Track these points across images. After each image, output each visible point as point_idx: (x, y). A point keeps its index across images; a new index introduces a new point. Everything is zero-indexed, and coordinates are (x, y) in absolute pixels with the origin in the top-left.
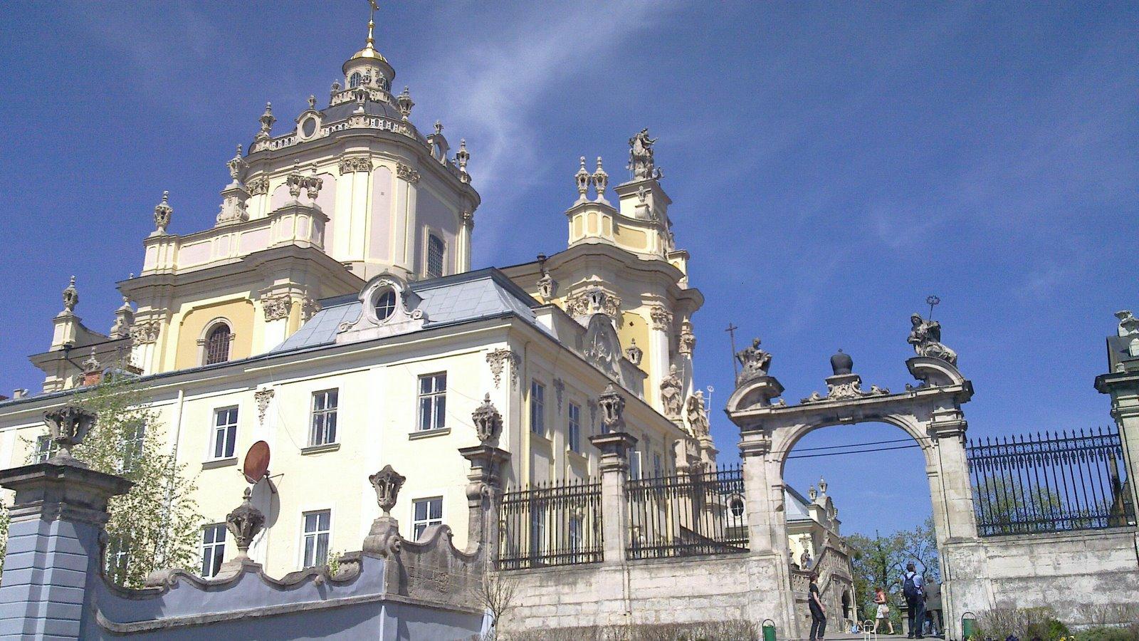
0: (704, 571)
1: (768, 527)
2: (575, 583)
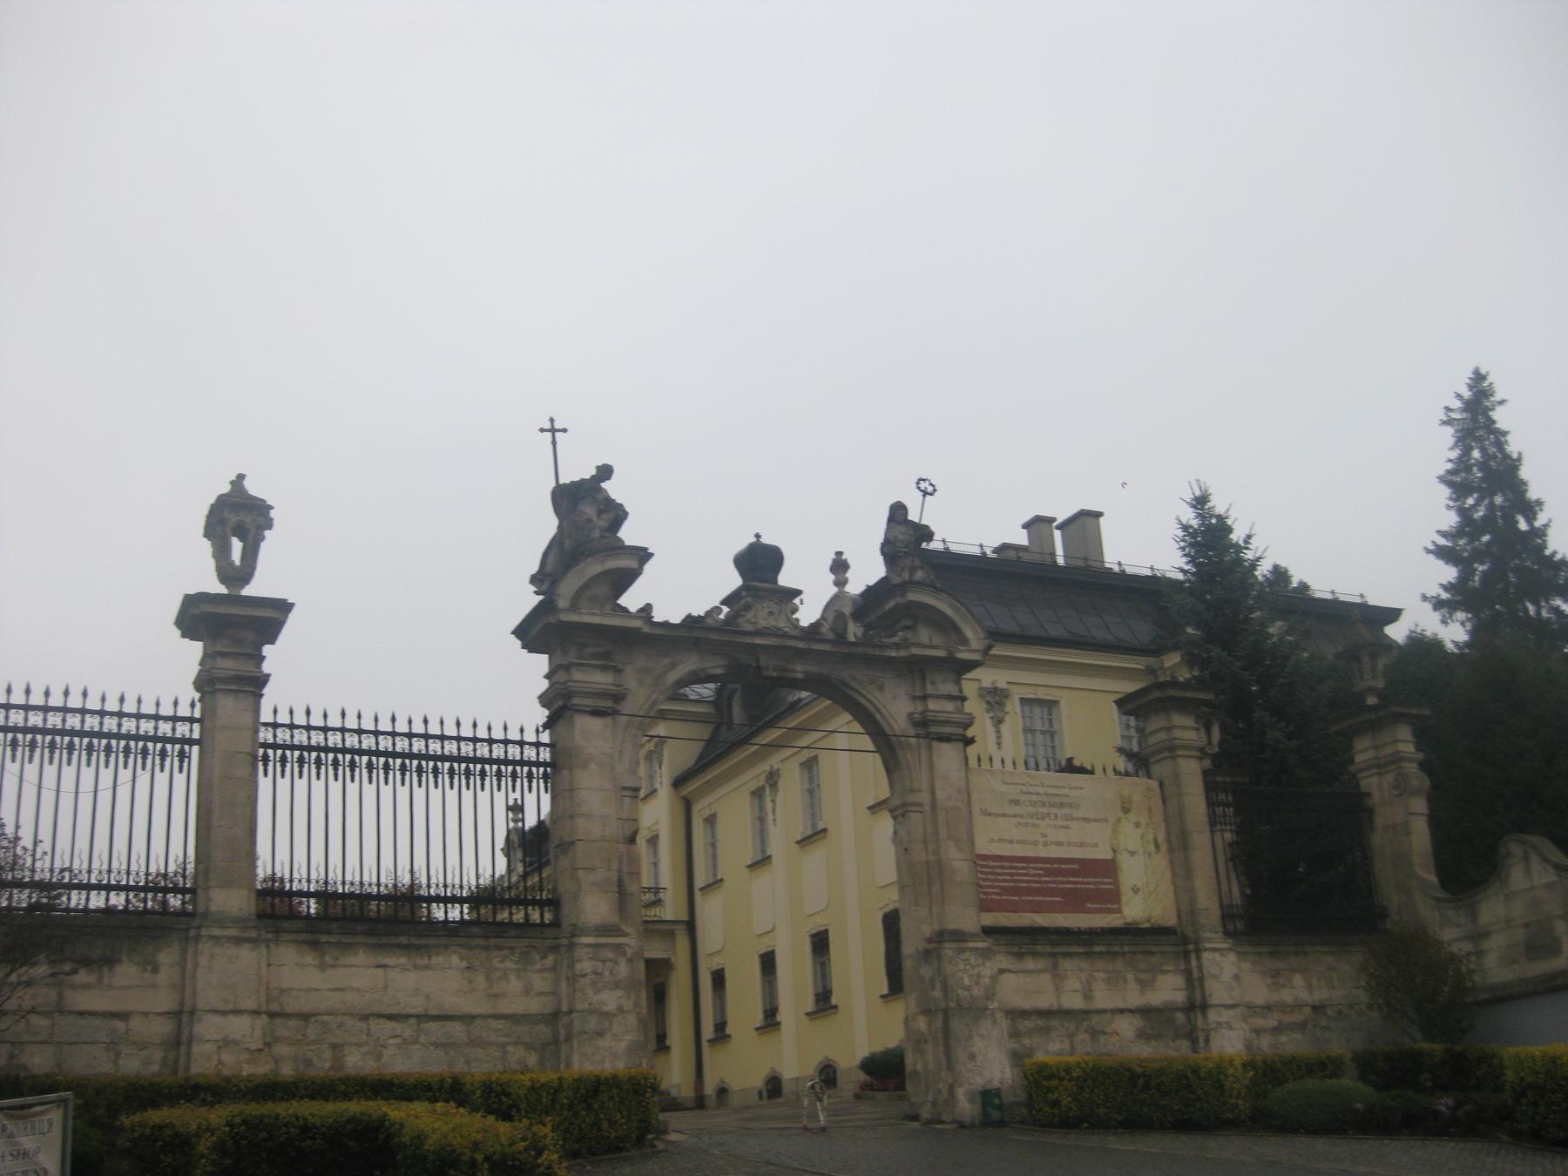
0: (455, 960)
1: (614, 876)
2: (110, 961)
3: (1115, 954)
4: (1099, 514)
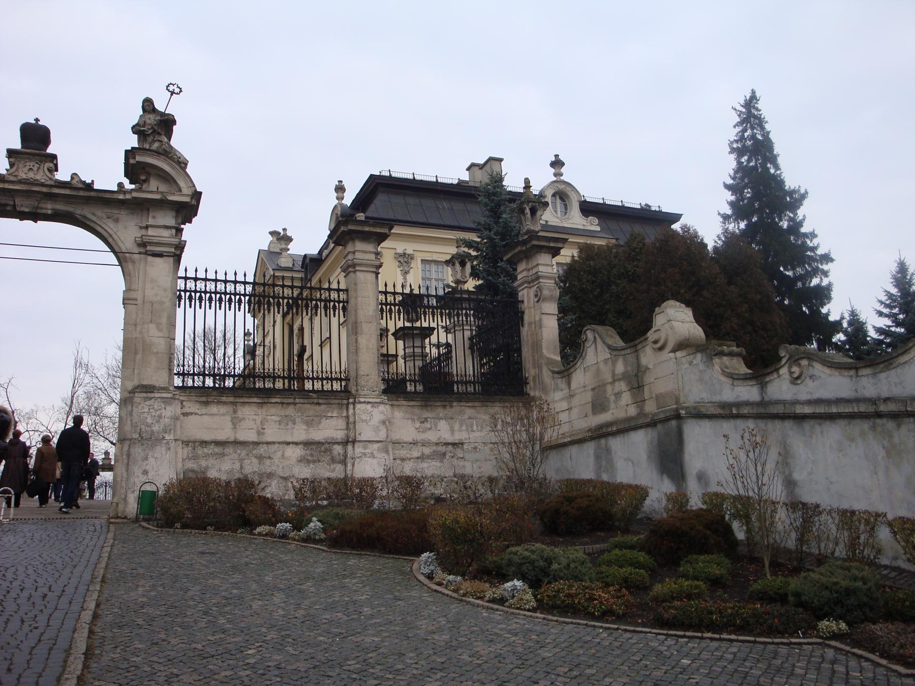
3: (288, 404)
4: (501, 160)
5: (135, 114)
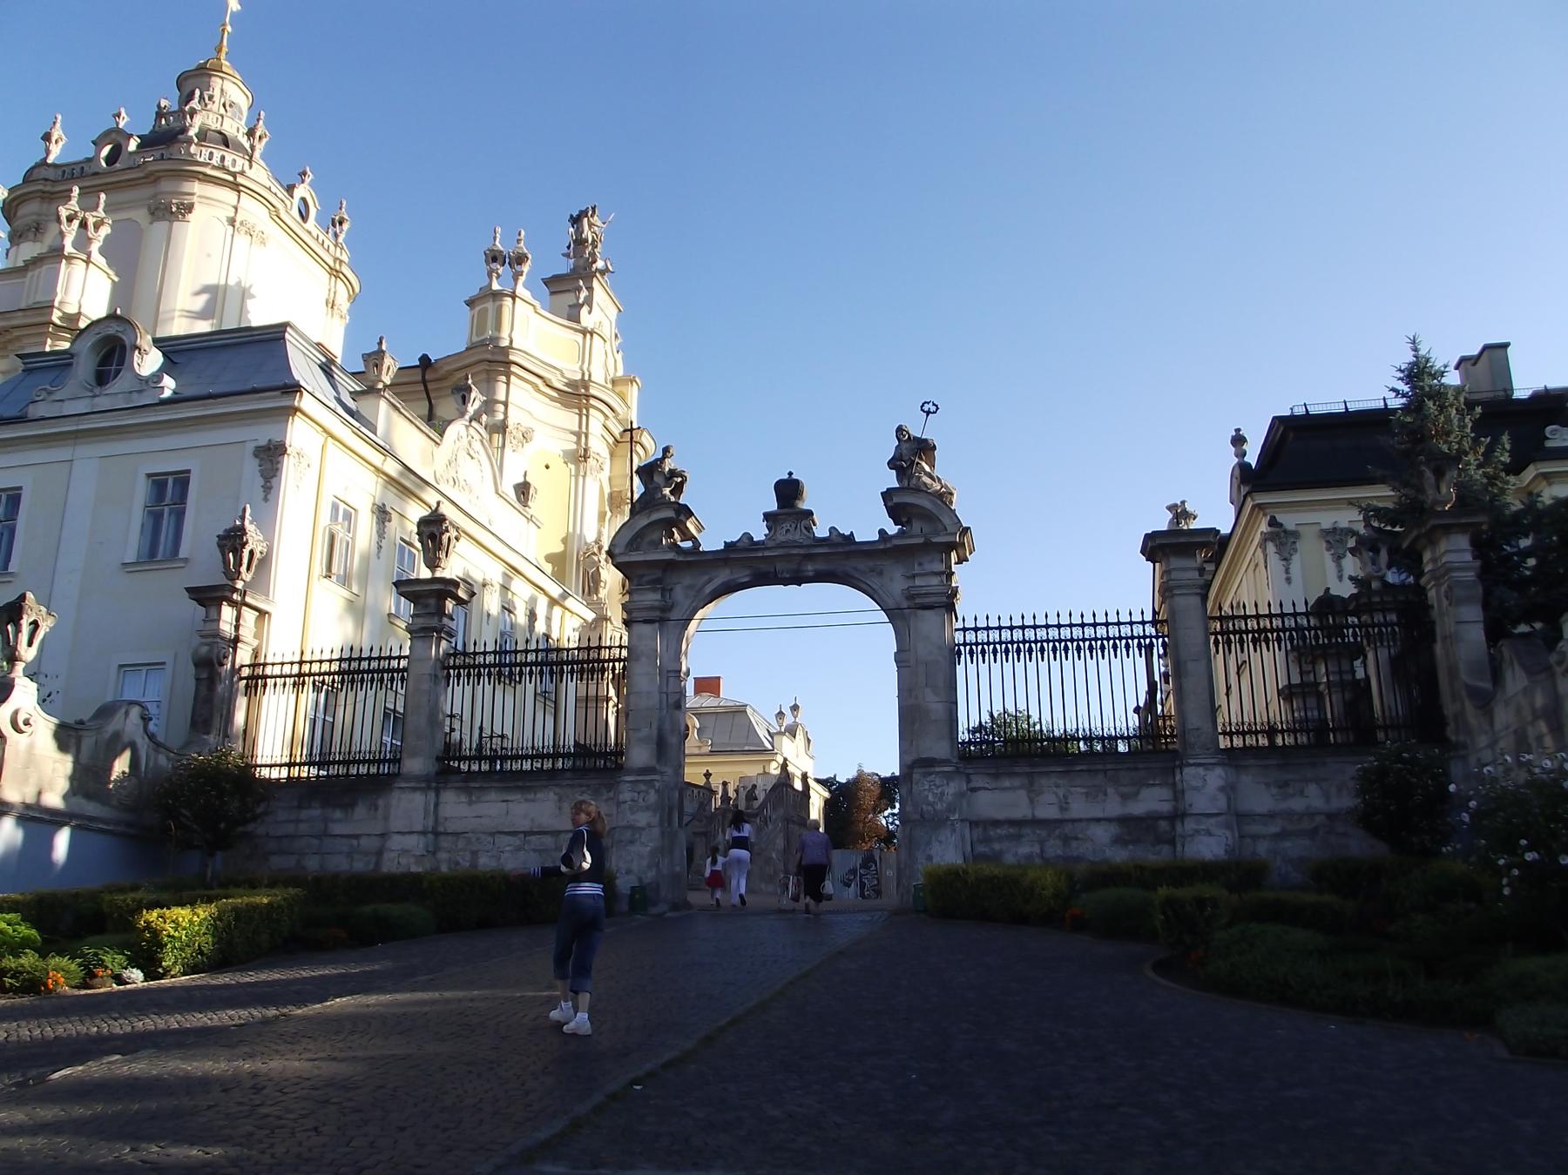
1: (655, 733)
2: (352, 805)
3: (1097, 771)
5: (890, 446)
